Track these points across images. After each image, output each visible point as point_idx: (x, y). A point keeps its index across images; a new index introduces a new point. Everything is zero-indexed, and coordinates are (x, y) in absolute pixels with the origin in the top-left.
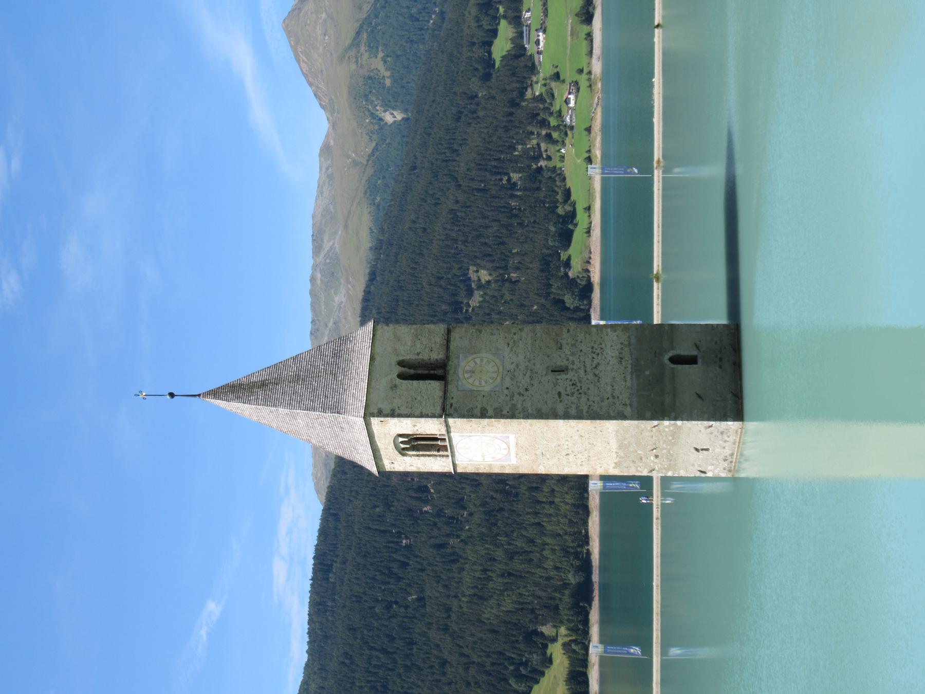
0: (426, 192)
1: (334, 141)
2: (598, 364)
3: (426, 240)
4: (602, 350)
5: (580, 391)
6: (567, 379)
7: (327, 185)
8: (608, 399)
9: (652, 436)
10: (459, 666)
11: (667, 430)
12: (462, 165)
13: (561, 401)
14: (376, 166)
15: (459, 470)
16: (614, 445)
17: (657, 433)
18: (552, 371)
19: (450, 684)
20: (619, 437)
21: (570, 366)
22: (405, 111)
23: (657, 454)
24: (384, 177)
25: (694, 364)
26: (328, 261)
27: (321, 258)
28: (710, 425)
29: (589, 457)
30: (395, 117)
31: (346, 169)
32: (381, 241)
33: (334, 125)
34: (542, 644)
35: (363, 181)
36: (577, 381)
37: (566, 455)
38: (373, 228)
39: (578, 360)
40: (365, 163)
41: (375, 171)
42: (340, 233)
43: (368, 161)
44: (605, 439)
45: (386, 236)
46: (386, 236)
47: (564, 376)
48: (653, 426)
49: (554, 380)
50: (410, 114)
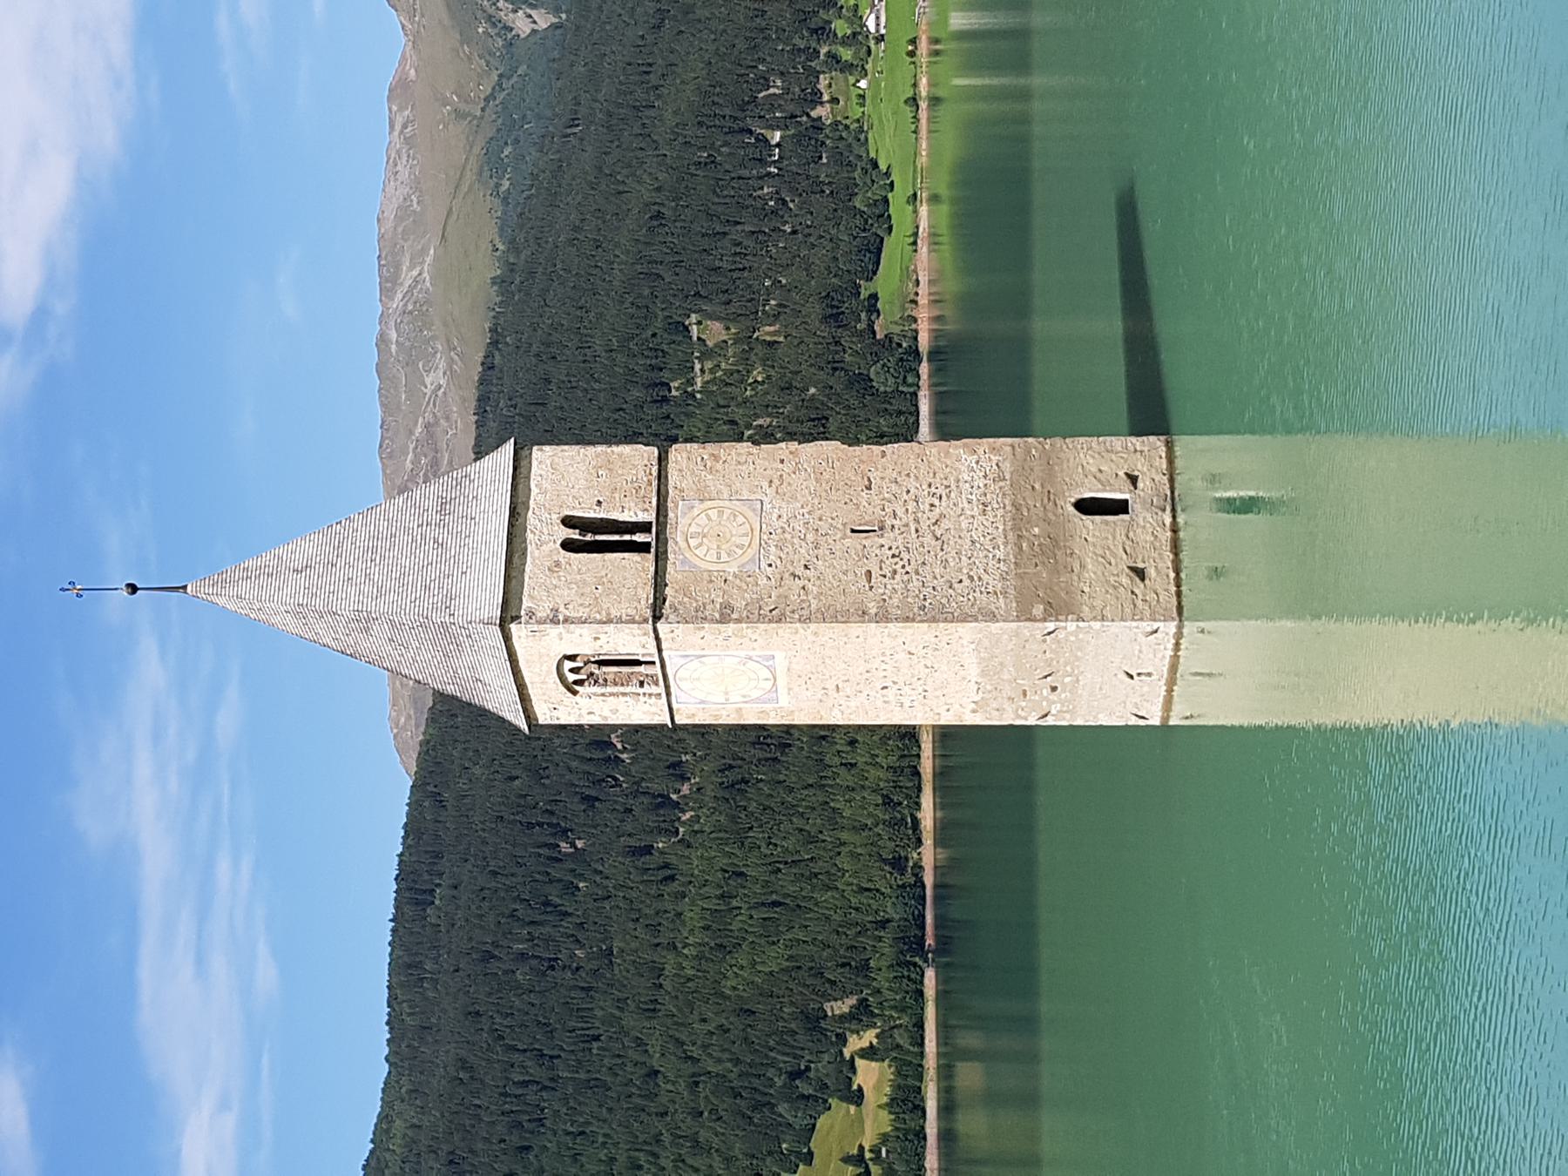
0: (600, 169)
1: (416, 71)
2: (942, 516)
3: (600, 264)
4: (948, 490)
5: (907, 569)
6: (883, 546)
7: (405, 158)
8: (961, 581)
9: (1045, 652)
10: (680, 1080)
11: (1073, 638)
12: (668, 115)
13: (871, 588)
14: (500, 121)
15: (679, 720)
16: (973, 672)
17: (1054, 646)
18: (853, 531)
19: (666, 1113)
20: (982, 655)
21: (889, 523)
22: (557, 11)
23: (1053, 685)
24: (517, 141)
25: (1123, 513)
26: (410, 307)
27: (397, 303)
28: (1155, 628)
29: (926, 691)
30: (535, 22)
31: (441, 127)
32: (511, 268)
33: (416, 40)
34: (837, 1035)
35: (477, 150)
36: (902, 548)
37: (883, 688)
38: (497, 241)
39: (904, 509)
40: (478, 113)
41: (499, 130)
42: (432, 252)
43: (483, 110)
44: (956, 658)
45: (523, 257)
46: (523, 257)
47: (871, 541)
48: (1046, 632)
49: (860, 547)
50: (564, 16)
